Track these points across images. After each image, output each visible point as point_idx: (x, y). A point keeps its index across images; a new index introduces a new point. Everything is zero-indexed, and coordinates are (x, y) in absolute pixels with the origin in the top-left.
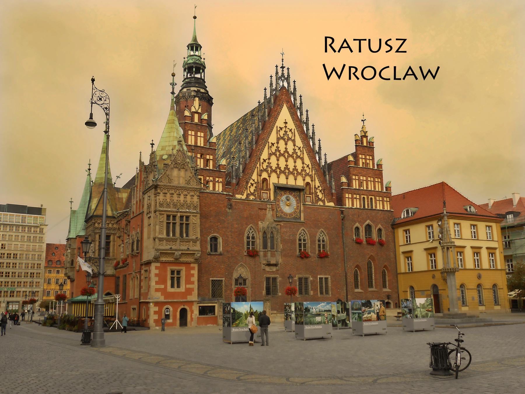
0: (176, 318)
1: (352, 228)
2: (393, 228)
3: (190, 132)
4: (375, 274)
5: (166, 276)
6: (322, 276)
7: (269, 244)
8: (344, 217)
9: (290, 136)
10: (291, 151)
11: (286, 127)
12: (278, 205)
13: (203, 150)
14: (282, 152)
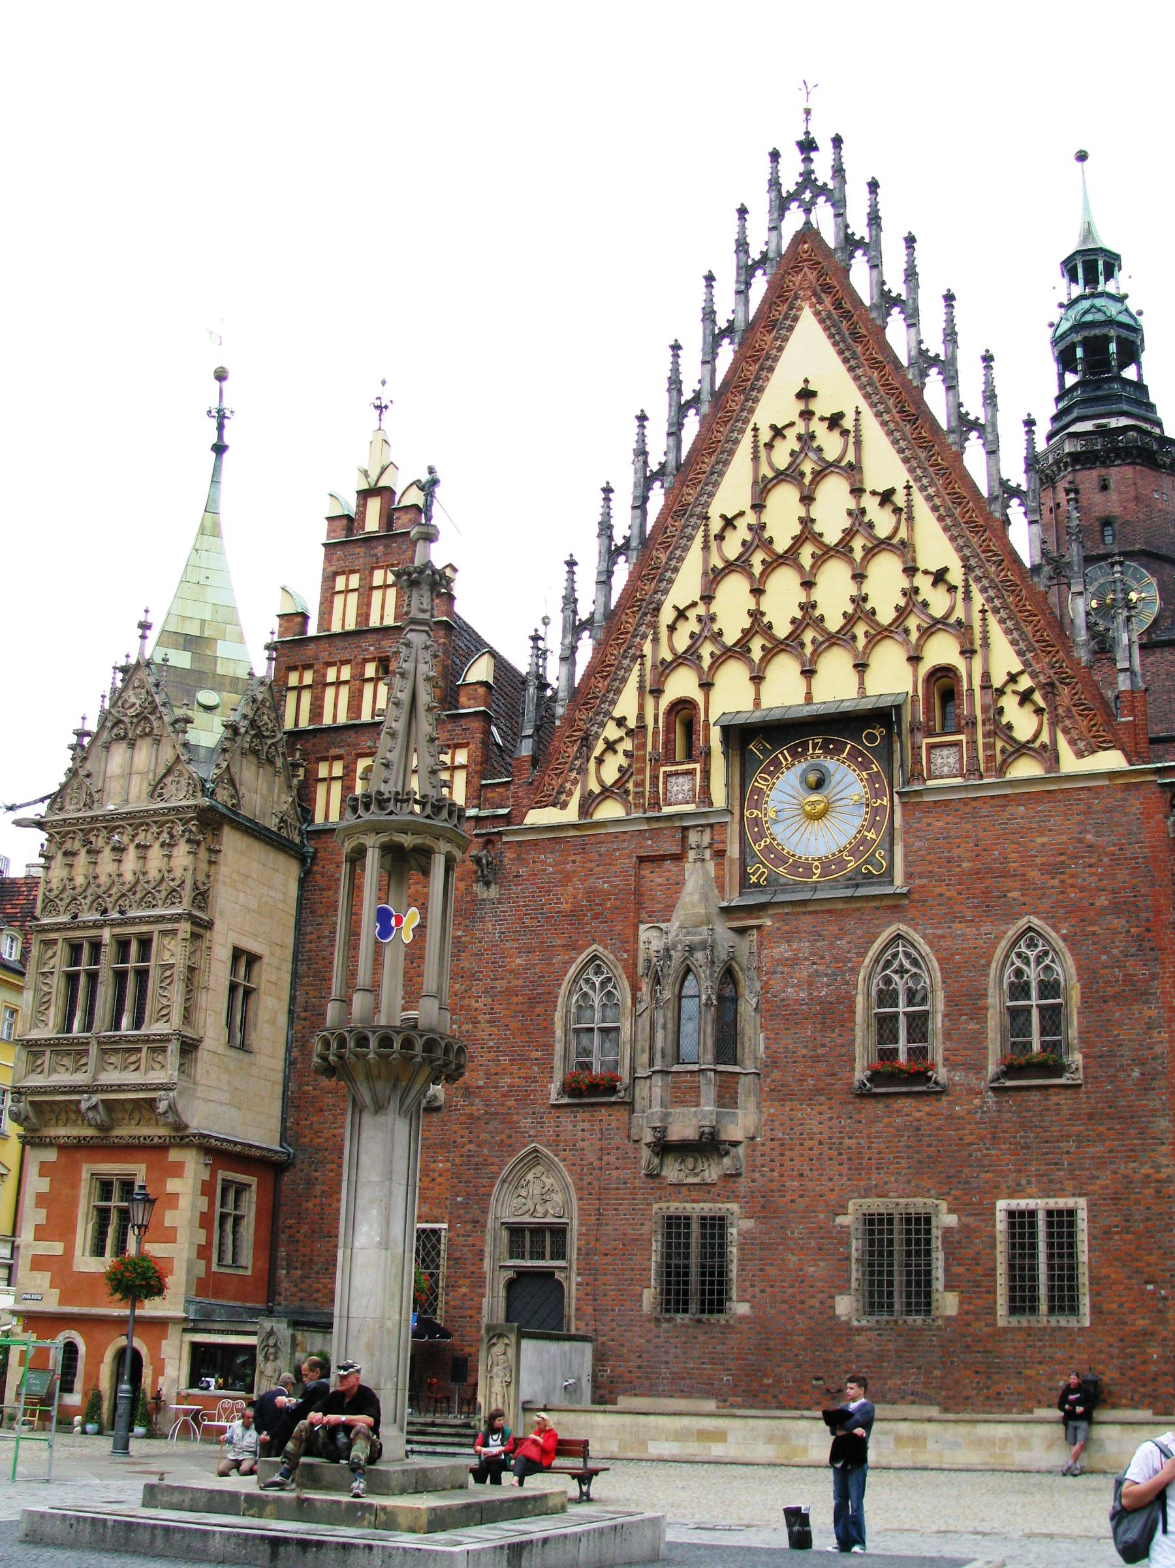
6: (1023, 1204)
11: (807, 415)
12: (756, 821)
13: (386, 643)
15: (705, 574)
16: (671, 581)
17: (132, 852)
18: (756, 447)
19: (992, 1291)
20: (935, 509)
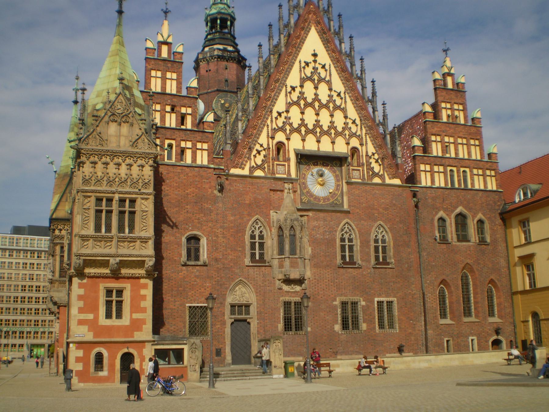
0: (114, 369)
1: (433, 219)
2: (503, 220)
3: (153, 73)
4: (475, 294)
5: (97, 299)
6: (381, 299)
7: (287, 247)
8: (418, 202)
9: (323, 75)
10: (324, 99)
11: (315, 61)
13: (175, 100)
14: (309, 100)
15: (286, 103)
16: (275, 103)
17: (124, 167)
18: (300, 67)
19: (374, 323)
20: (351, 100)
